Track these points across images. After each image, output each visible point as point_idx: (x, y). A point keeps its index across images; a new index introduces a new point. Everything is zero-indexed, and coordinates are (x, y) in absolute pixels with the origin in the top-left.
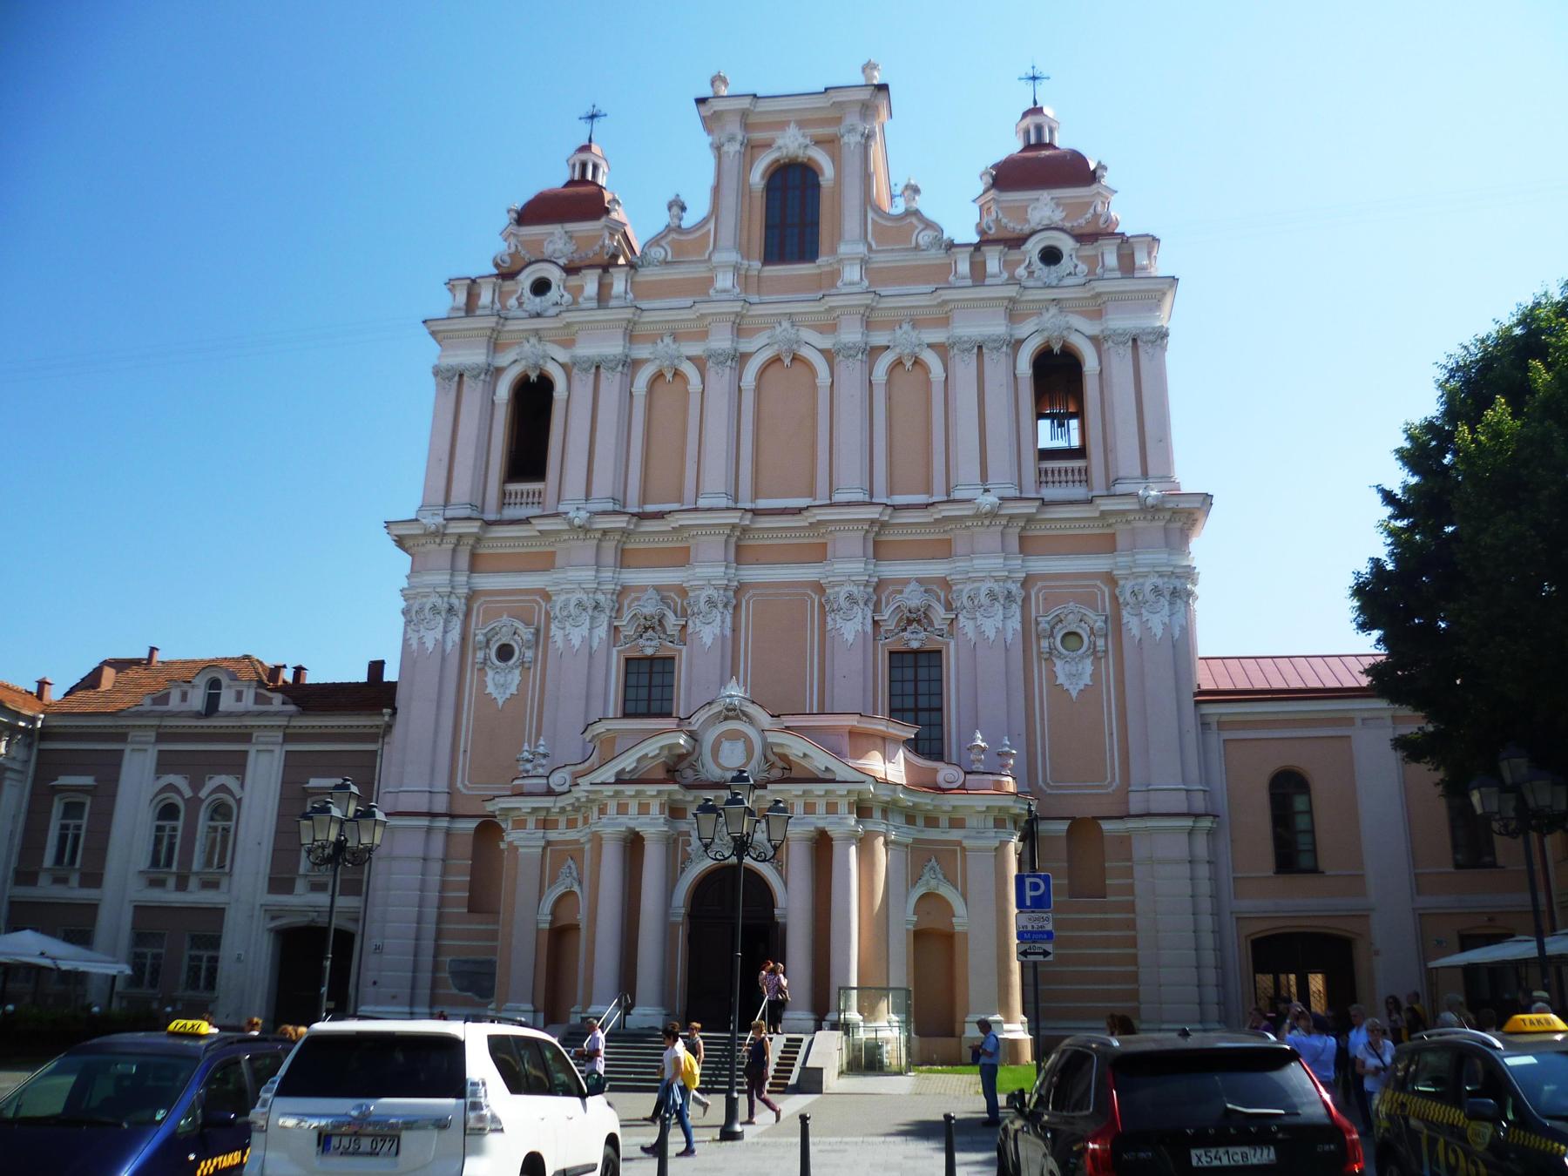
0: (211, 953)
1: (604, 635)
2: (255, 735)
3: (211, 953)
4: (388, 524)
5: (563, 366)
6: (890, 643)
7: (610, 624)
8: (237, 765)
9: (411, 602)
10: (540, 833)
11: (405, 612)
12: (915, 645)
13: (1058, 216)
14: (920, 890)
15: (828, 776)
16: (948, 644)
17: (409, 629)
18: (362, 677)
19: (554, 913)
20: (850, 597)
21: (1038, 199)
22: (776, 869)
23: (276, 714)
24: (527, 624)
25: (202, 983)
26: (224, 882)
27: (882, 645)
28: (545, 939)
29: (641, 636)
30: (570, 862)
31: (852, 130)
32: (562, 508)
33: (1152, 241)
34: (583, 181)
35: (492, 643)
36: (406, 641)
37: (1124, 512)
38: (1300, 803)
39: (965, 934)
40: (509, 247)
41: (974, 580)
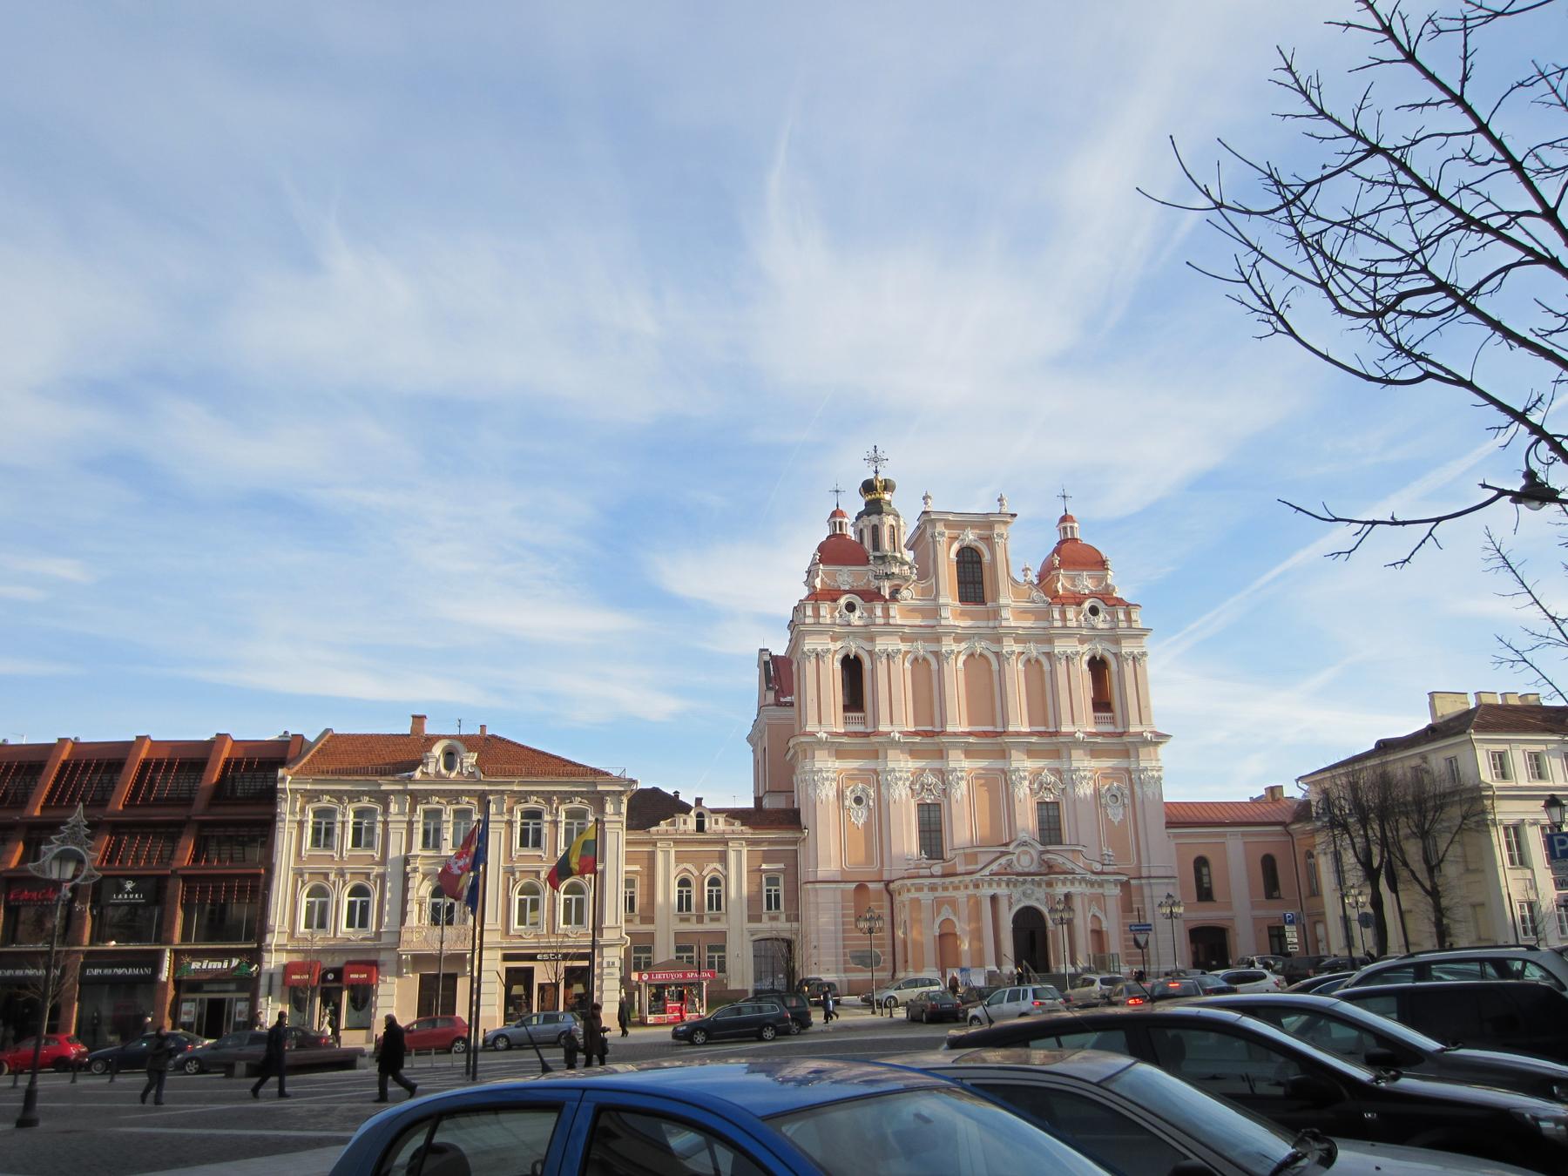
0: (721, 954)
14: (1091, 913)
25: (1129, 959)
26: (723, 918)
30: (946, 906)
38: (1205, 871)
39: (1107, 932)
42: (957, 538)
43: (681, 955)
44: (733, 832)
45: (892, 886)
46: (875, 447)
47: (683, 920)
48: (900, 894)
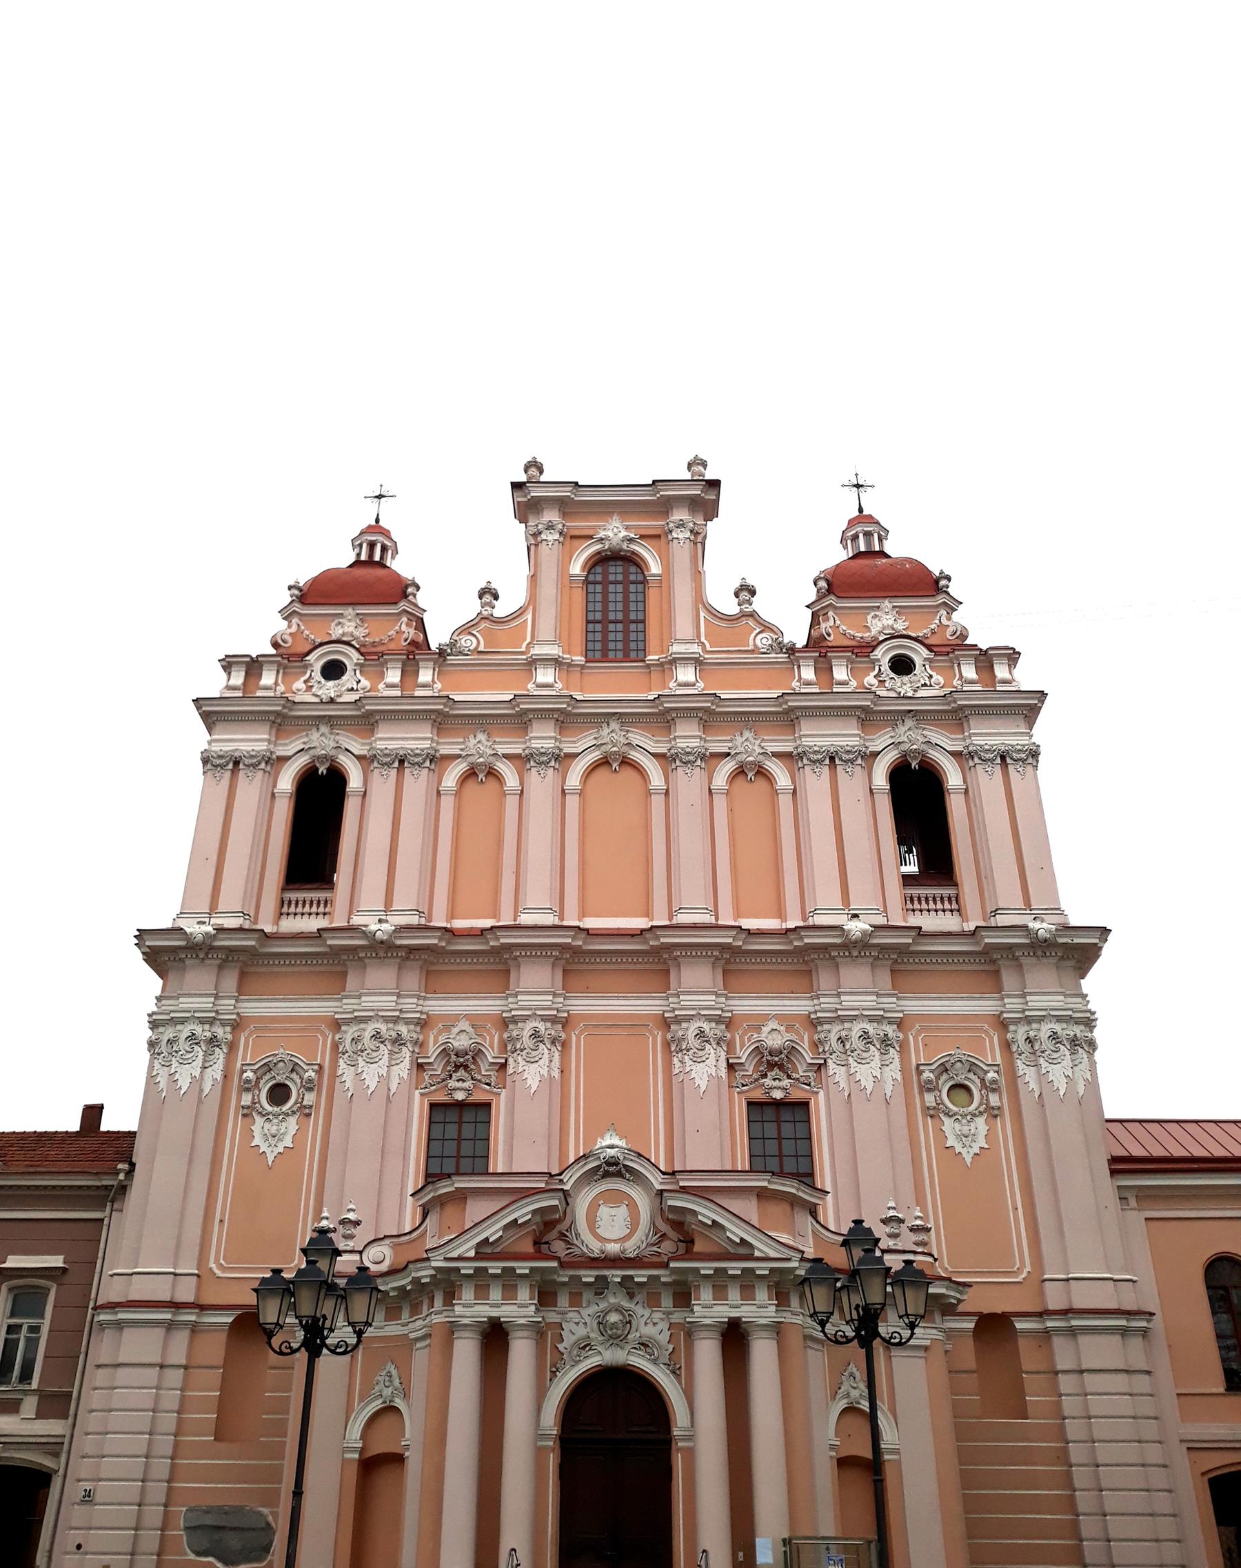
1: (405, 1074)
4: (142, 935)
5: (359, 757)
6: (747, 1091)
7: (411, 1063)
9: (161, 1029)
11: (152, 1044)
12: (778, 1095)
13: (900, 626)
14: (843, 1404)
15: (742, 1251)
16: (817, 1093)
18: (74, 1125)
19: (364, 1436)
20: (701, 1034)
21: (878, 607)
22: (674, 1372)
27: (738, 1093)
28: (353, 1473)
29: (451, 1076)
31: (681, 525)
32: (357, 920)
33: (1012, 656)
34: (370, 562)
35: (262, 1082)
36: (151, 1078)
37: (1011, 947)
40: (289, 627)
41: (842, 1019)
42: (591, 537)
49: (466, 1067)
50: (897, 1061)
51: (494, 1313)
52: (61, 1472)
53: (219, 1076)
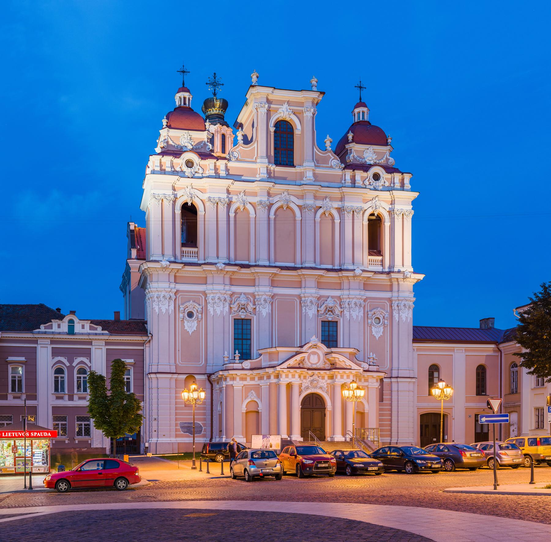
0: (86, 423)
1: (227, 310)
2: (93, 342)
3: (86, 423)
6: (322, 318)
8: (87, 353)
10: (241, 382)
16: (340, 320)
17: (154, 304)
23: (99, 334)
24: (199, 305)
30: (253, 391)
43: (57, 422)
44: (96, 334)
45: (213, 377)
46: (215, 74)
47: (58, 398)
48: (218, 383)
49: (244, 309)
50: (362, 312)
51: (290, 381)
52: (145, 414)
53: (173, 309)
